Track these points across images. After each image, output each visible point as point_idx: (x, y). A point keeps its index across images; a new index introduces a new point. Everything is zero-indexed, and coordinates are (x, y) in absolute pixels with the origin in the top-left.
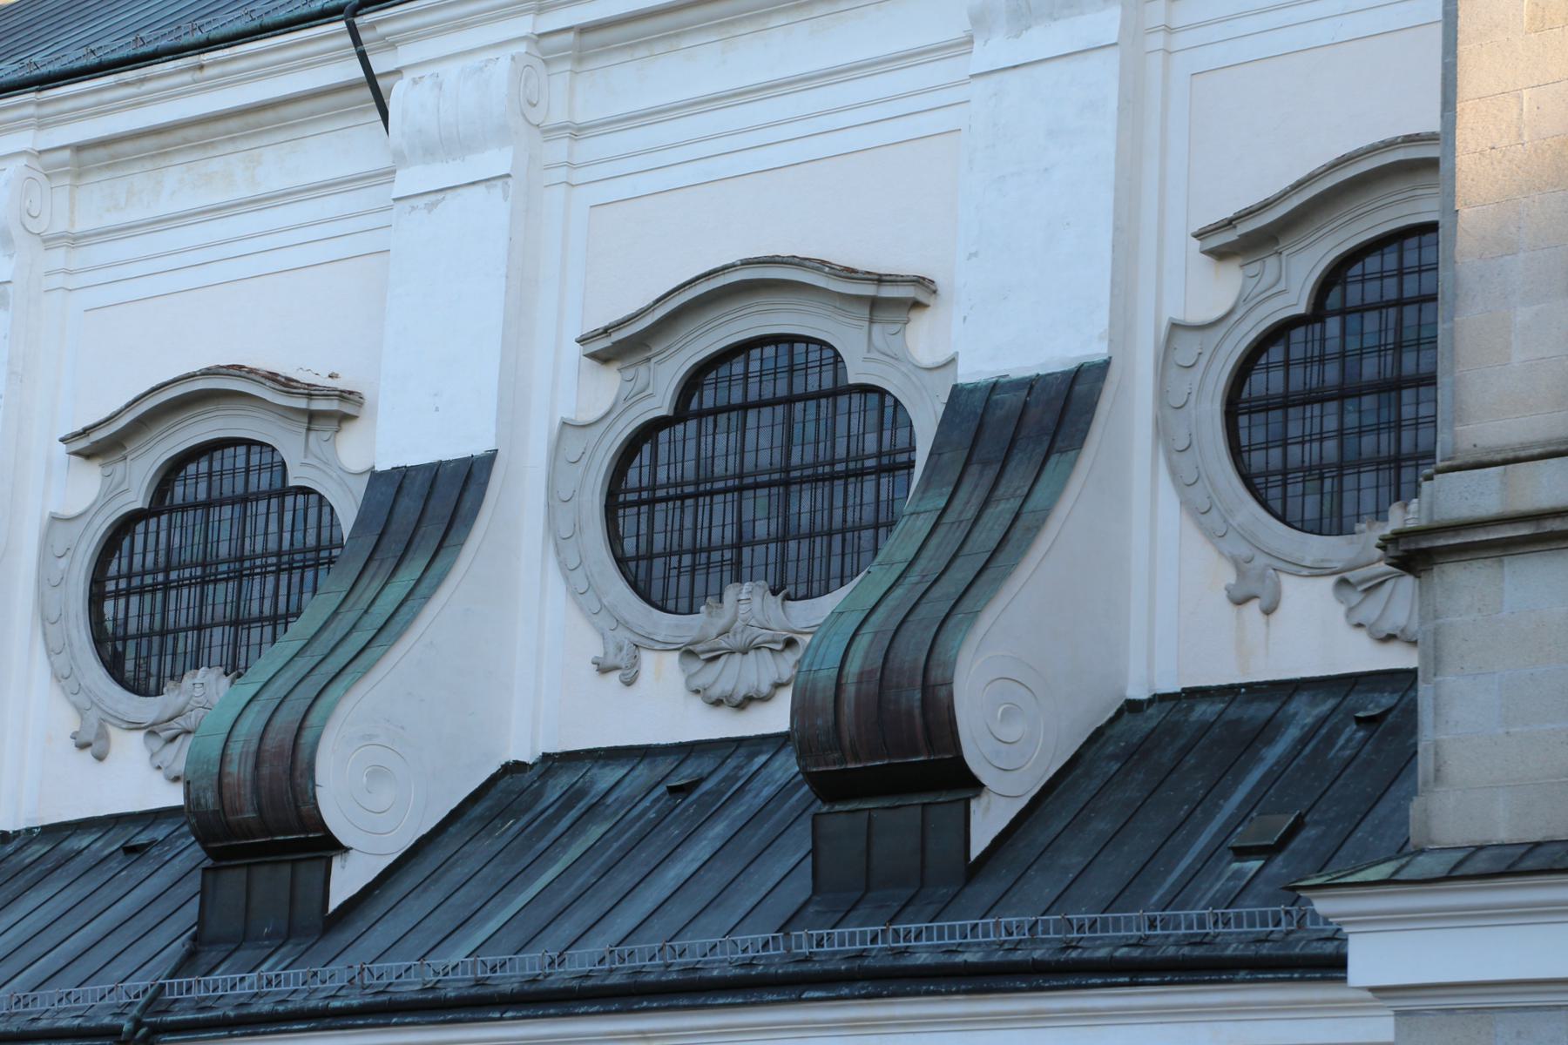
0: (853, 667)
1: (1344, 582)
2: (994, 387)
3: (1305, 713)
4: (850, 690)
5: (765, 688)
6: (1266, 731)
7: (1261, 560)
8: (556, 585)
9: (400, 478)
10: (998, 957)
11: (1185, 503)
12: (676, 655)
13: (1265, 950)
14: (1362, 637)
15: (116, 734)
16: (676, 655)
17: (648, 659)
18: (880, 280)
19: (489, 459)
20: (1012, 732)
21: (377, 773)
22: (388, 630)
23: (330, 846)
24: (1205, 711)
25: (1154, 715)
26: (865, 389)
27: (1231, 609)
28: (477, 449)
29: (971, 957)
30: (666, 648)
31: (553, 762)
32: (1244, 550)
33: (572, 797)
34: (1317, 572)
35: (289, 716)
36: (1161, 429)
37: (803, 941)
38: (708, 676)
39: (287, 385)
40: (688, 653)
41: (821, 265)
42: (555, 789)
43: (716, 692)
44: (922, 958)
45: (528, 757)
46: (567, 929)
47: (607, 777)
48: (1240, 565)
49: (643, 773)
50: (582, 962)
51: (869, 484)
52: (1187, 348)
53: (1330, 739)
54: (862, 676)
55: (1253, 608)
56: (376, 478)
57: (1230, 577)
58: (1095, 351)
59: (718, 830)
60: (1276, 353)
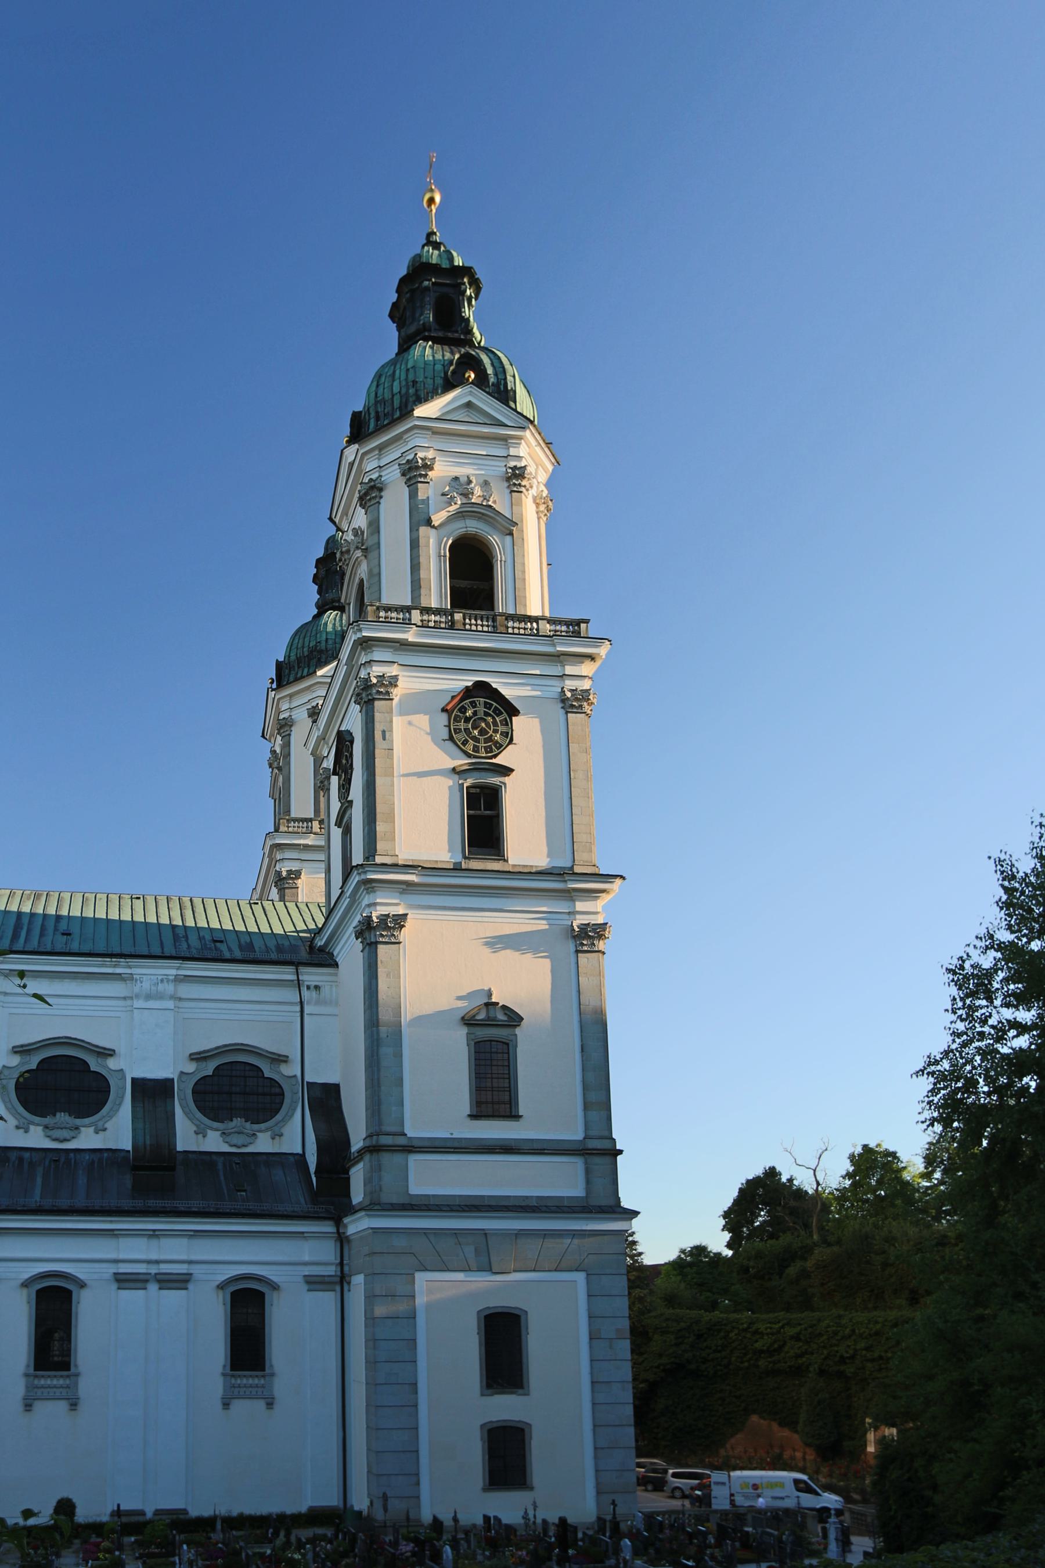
1: (224, 1133)
5: (68, 1138)
7: (202, 1126)
10: (202, 1210)
12: (41, 1128)
16: (41, 1128)
17: (32, 1127)
18: (105, 1049)
27: (194, 1136)
29: (194, 1209)
30: (38, 1125)
34: (217, 1130)
38: (51, 1133)
40: (46, 1127)
41: (83, 1041)
43: (54, 1137)
48: (197, 1126)
52: (184, 1078)
54: (151, 1145)
55: (200, 1136)
57: (195, 1128)
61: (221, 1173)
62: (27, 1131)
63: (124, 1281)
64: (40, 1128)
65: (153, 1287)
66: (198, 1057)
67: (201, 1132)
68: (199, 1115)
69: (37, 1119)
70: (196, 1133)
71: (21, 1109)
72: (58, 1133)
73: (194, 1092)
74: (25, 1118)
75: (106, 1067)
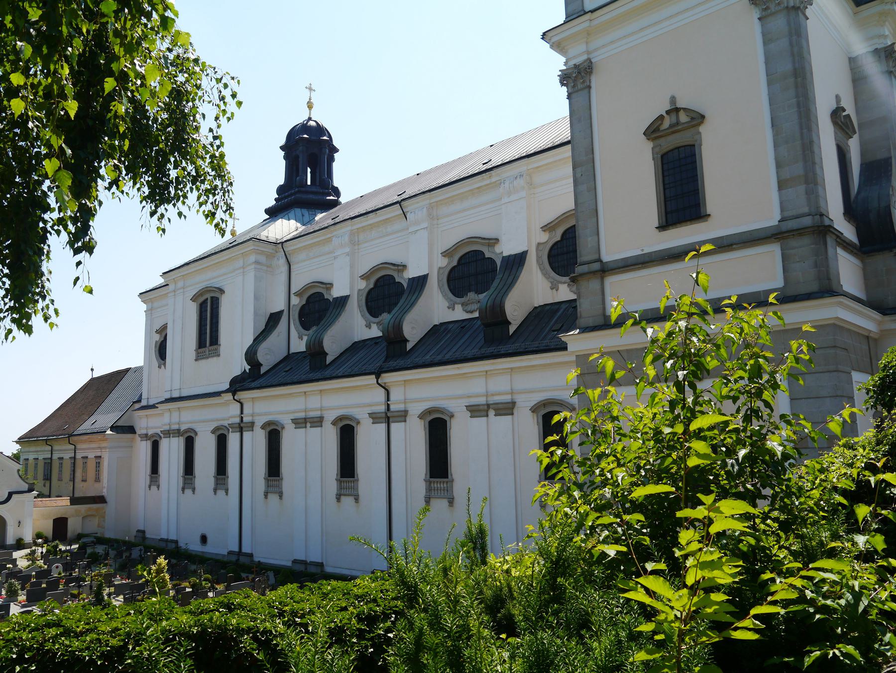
0: (488, 305)
2: (509, 256)
3: (564, 307)
4: (488, 309)
6: (557, 310)
8: (440, 295)
9: (414, 279)
10: (515, 351)
11: (542, 273)
13: (558, 346)
14: (572, 293)
15: (372, 324)
19: (428, 274)
20: (515, 314)
21: (413, 328)
22: (413, 305)
23: (406, 341)
24: (548, 307)
25: (538, 310)
26: (488, 258)
28: (426, 273)
30: (459, 304)
31: (442, 324)
32: (552, 280)
33: (445, 329)
35: (319, 335)
36: (537, 261)
37: (483, 351)
39: (394, 265)
40: (462, 305)
42: (442, 329)
44: (503, 352)
45: (437, 324)
46: (445, 352)
47: (451, 326)
49: (457, 325)
50: (447, 357)
51: (490, 274)
53: (568, 311)
55: (554, 290)
56: (409, 279)
58: (525, 249)
59: (469, 333)
60: (555, 247)
61: (556, 318)
62: (453, 309)
63: (476, 411)
64: (460, 306)
65: (492, 413)
66: (546, 228)
67: (554, 287)
68: (553, 274)
69: (458, 300)
70: (552, 289)
71: (450, 295)
72: (469, 308)
73: (549, 256)
74: (451, 300)
75: (494, 253)
